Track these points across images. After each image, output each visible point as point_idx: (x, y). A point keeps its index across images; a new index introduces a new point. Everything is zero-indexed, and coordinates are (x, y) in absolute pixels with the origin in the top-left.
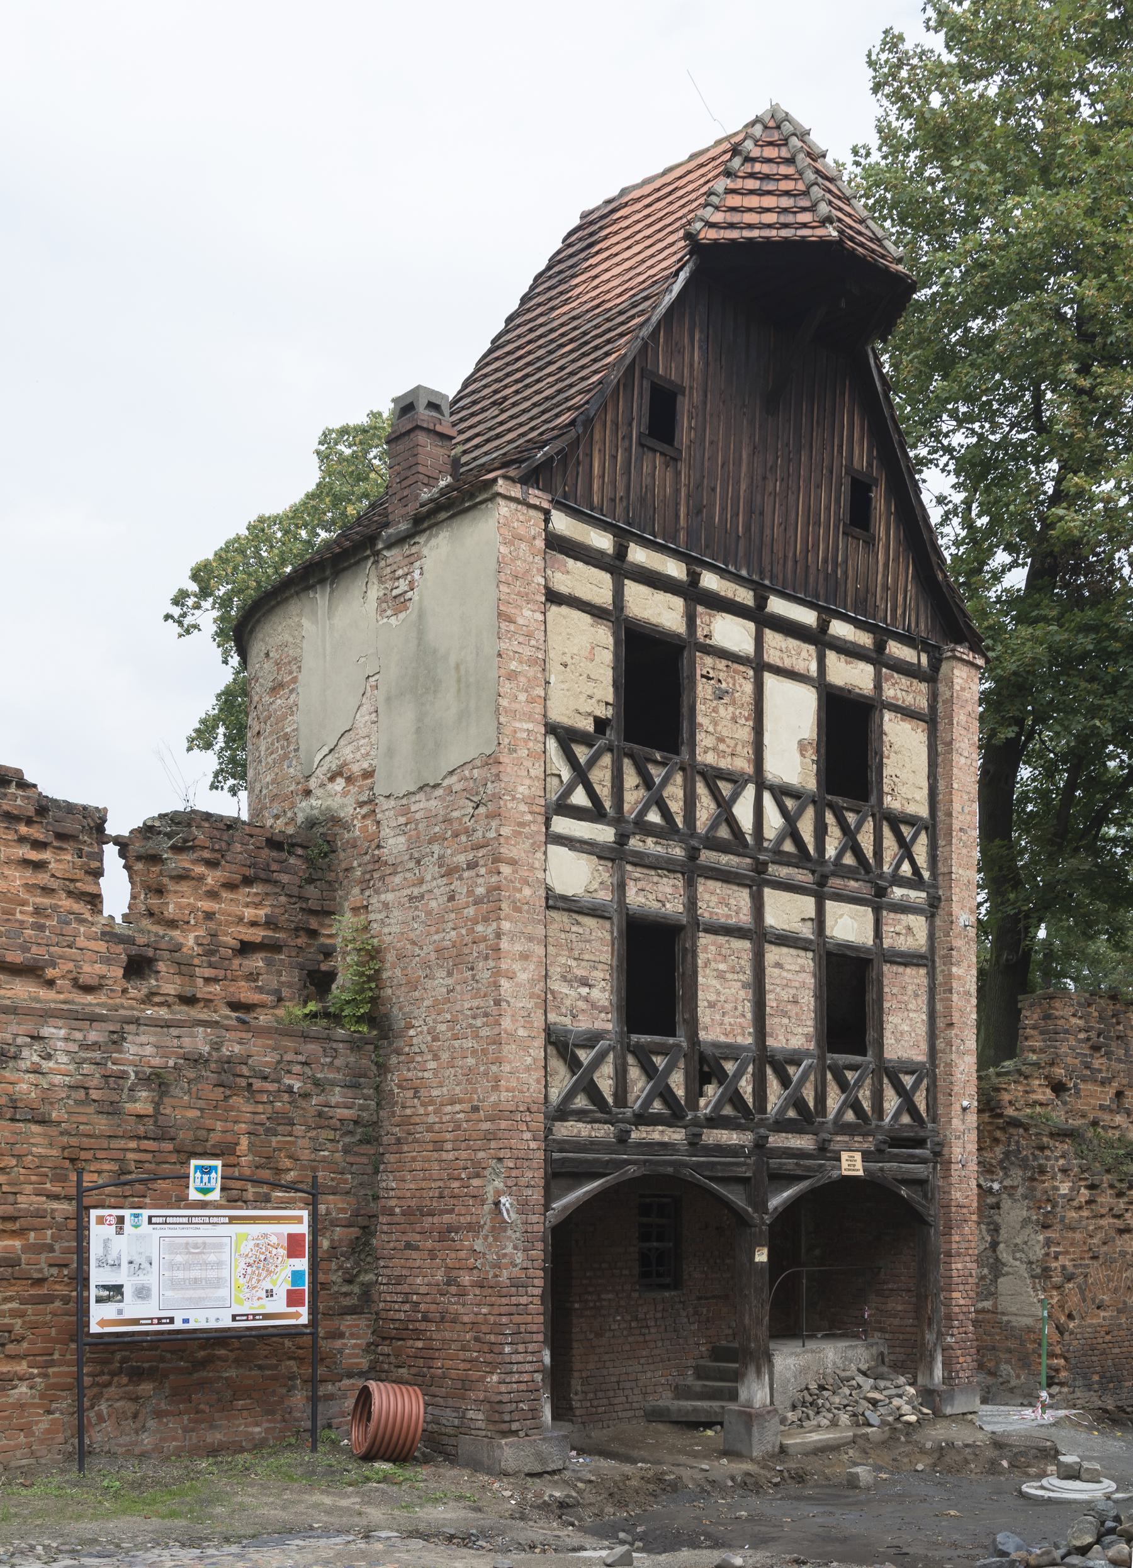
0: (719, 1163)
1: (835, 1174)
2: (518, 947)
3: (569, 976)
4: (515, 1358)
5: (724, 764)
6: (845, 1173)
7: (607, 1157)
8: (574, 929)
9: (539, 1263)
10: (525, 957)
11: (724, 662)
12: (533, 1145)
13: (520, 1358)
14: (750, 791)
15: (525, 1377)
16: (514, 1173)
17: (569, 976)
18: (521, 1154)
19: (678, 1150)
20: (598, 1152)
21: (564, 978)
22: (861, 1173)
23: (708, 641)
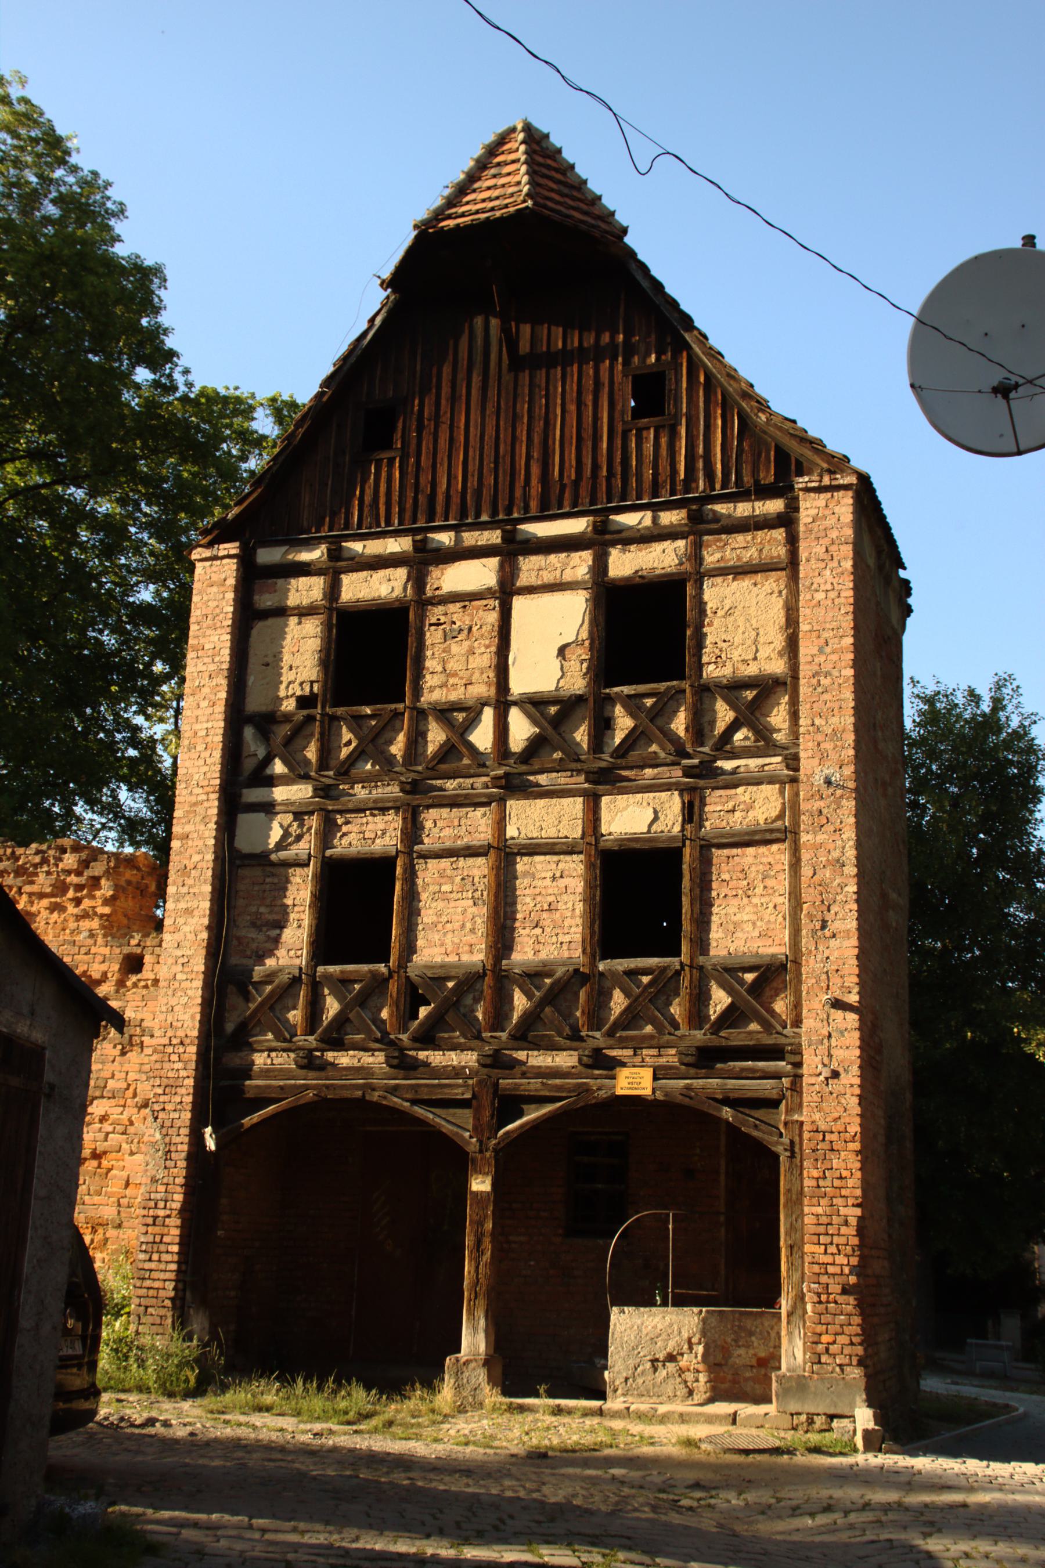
0: (426, 1085)
1: (603, 1094)
2: (182, 905)
3: (259, 923)
4: (148, 1265)
5: (453, 696)
6: (619, 1092)
7: (281, 1083)
8: (268, 880)
9: (180, 1180)
10: (189, 912)
11: (458, 605)
12: (183, 1073)
13: (152, 1265)
14: (488, 715)
15: (157, 1284)
16: (162, 1099)
17: (259, 923)
18: (171, 1082)
19: (373, 1074)
20: (275, 1078)
21: (253, 925)
22: (648, 1092)
23: (437, 593)
